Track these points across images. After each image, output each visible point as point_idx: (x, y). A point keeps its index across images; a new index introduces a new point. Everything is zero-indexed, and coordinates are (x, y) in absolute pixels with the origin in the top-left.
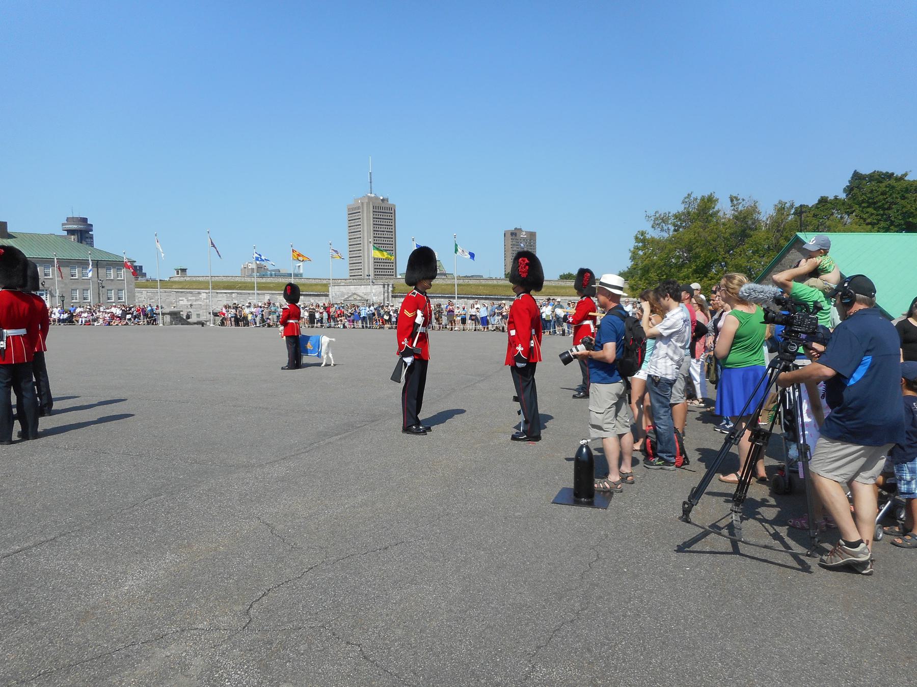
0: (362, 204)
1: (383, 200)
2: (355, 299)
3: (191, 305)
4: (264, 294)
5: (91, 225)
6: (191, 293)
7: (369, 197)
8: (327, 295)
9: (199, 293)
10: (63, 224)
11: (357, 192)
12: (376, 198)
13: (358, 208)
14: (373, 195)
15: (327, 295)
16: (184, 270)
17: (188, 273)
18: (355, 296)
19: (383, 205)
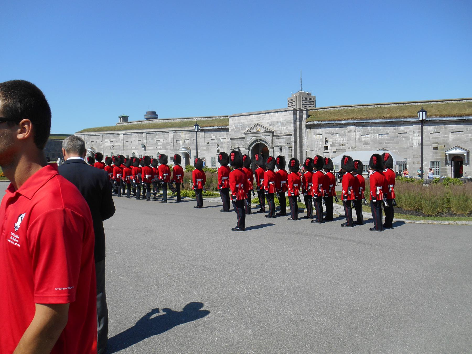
0: (296, 97)
1: (308, 94)
2: (258, 132)
3: (113, 147)
4: (168, 132)
5: (157, 115)
6: (112, 134)
7: (300, 93)
8: (227, 130)
9: (118, 134)
10: (145, 115)
11: (293, 91)
12: (304, 93)
13: (294, 99)
14: (302, 92)
15: (227, 130)
16: (125, 119)
17: (129, 120)
18: (258, 128)
19: (309, 97)
